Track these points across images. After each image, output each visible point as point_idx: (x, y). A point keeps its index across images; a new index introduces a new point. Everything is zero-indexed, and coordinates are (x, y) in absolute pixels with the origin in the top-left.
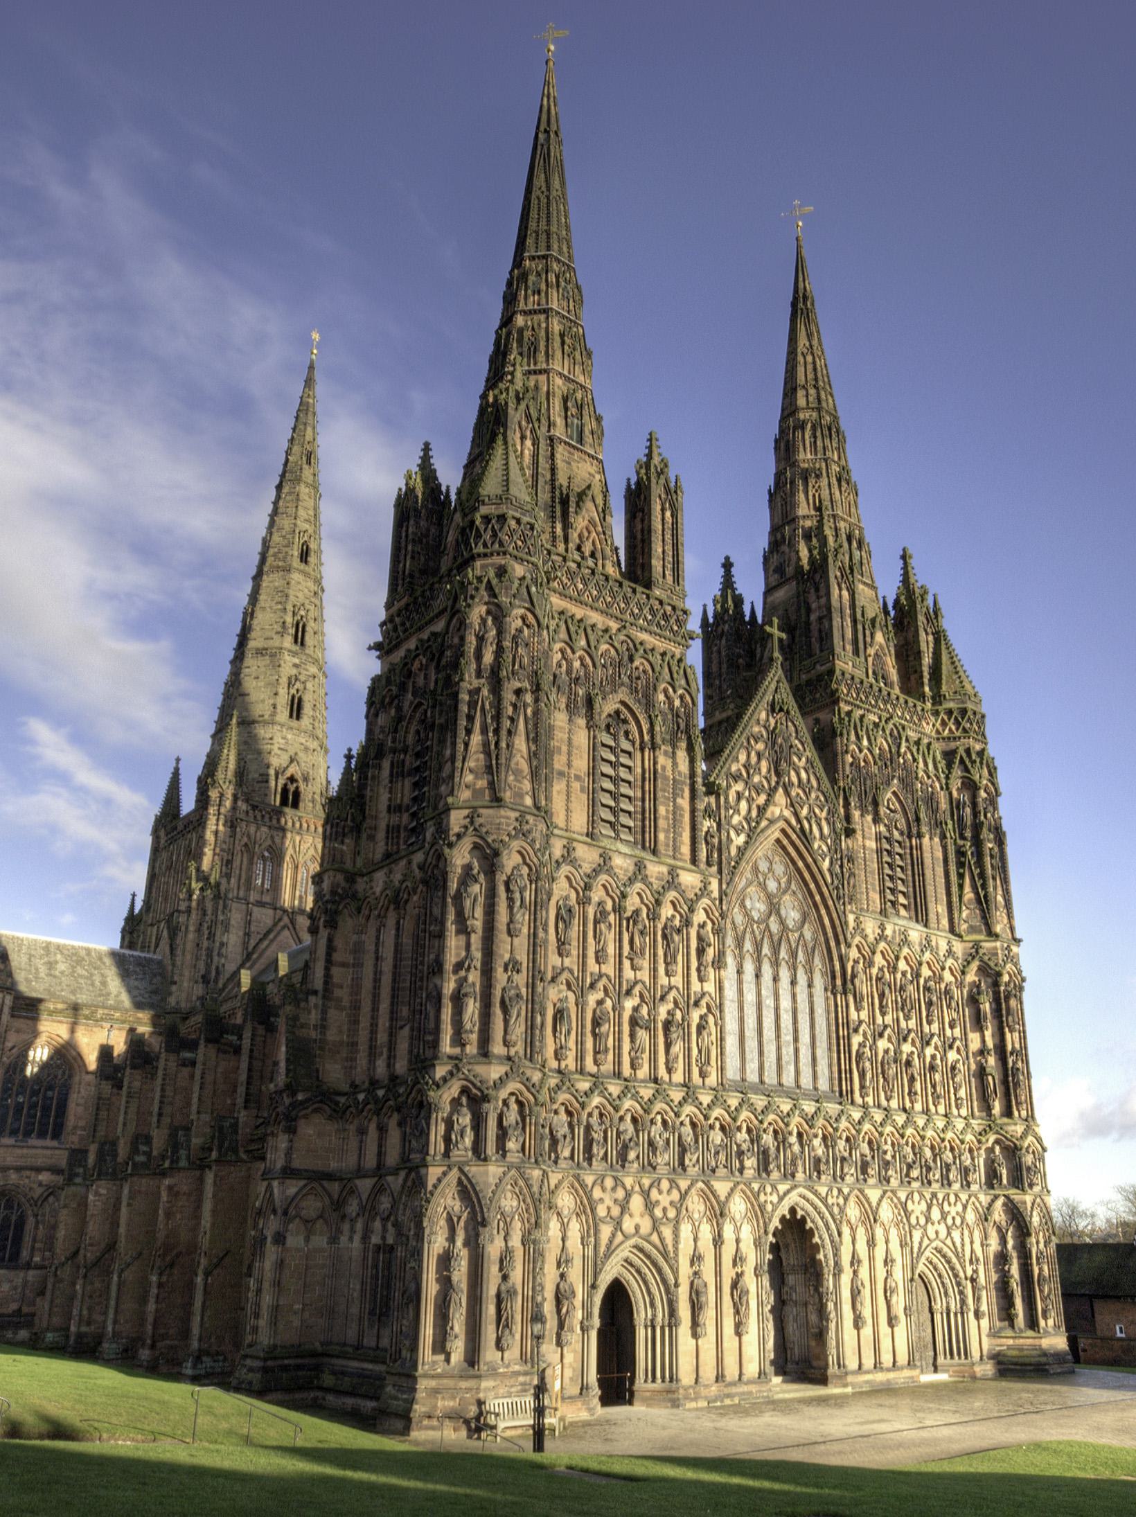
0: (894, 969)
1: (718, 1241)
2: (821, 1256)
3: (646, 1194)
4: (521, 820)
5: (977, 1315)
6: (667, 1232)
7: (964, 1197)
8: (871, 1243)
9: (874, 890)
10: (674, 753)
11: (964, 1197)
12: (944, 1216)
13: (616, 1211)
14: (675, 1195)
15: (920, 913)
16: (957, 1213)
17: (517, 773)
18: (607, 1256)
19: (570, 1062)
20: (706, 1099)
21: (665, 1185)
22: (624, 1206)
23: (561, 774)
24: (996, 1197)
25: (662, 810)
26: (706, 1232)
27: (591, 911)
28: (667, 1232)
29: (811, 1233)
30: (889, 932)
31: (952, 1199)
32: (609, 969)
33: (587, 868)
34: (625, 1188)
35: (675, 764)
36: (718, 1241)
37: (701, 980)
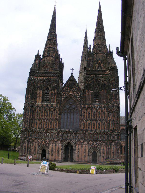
0: (92, 111)
1: (56, 146)
2: (73, 148)
3: (45, 141)
4: (29, 104)
5: (103, 157)
6: (48, 145)
7: (101, 141)
8: (82, 147)
9: (90, 100)
10: (54, 90)
11: (101, 141)
12: (96, 144)
13: (41, 142)
14: (49, 141)
15: (100, 102)
16: (100, 143)
17: (29, 99)
18: (40, 146)
19: (38, 127)
20: (54, 130)
21: (48, 140)
22: (42, 141)
23: (38, 97)
24: (108, 141)
25: (52, 98)
26: (54, 145)
27: (41, 111)
28: (48, 145)
29: (72, 145)
30: (91, 106)
31: (99, 141)
32: (43, 117)
33: (40, 107)
34: (42, 140)
35: (55, 92)
36: (56, 146)
37: (56, 117)
